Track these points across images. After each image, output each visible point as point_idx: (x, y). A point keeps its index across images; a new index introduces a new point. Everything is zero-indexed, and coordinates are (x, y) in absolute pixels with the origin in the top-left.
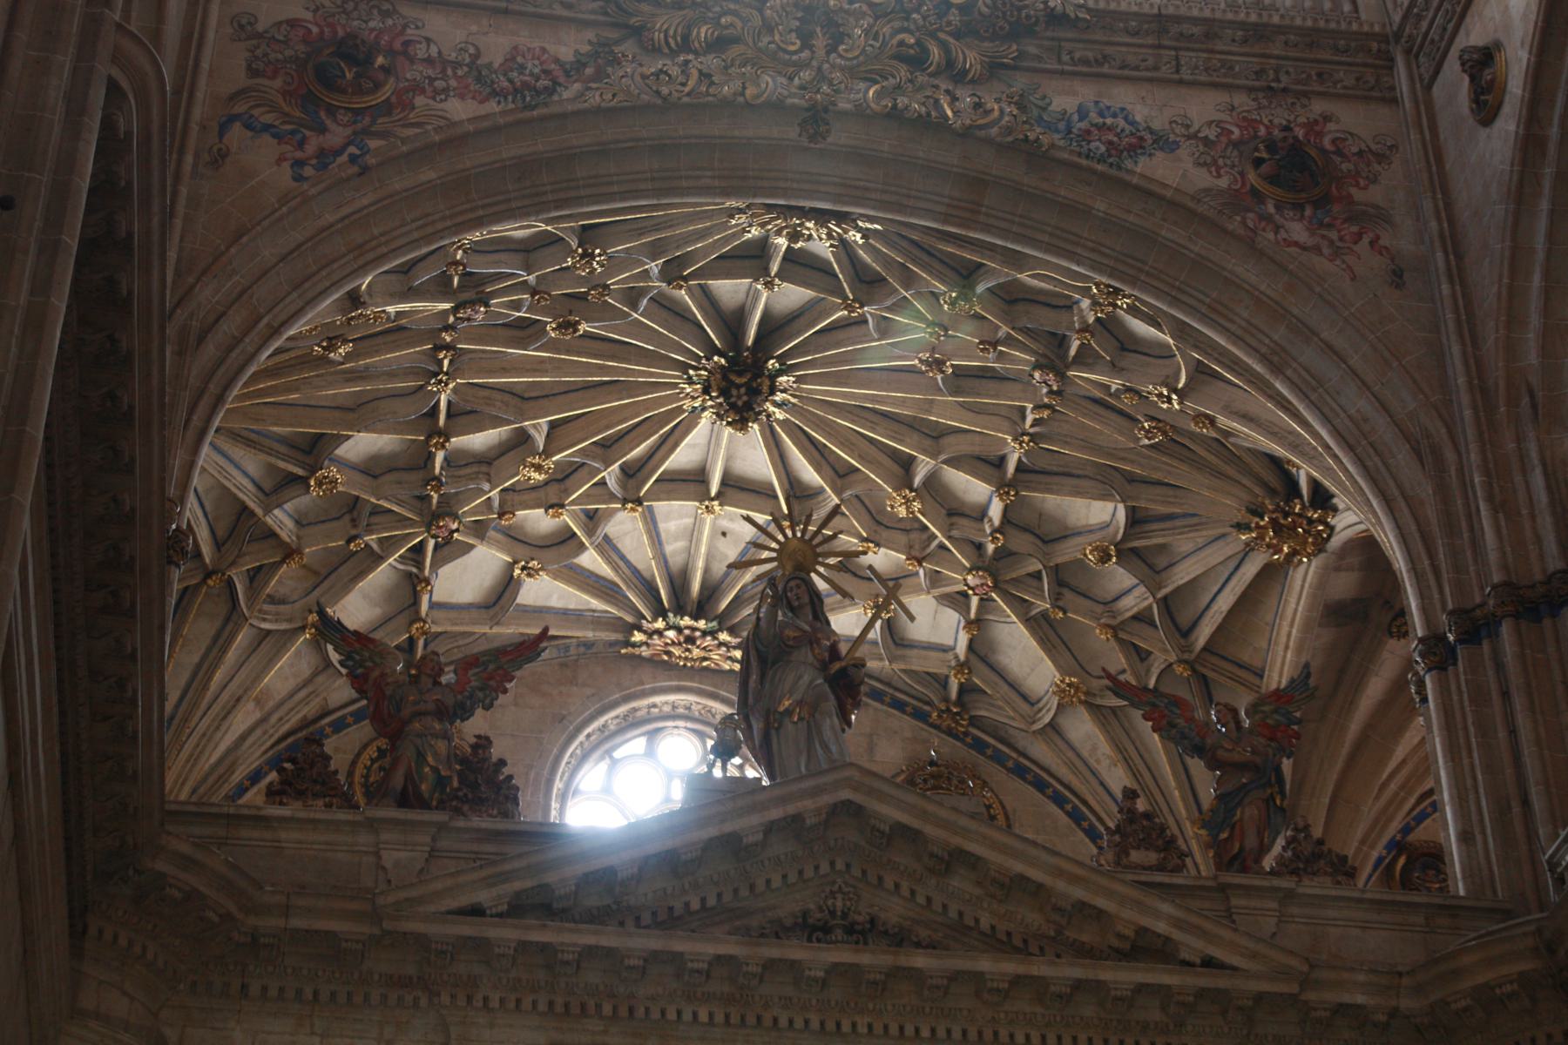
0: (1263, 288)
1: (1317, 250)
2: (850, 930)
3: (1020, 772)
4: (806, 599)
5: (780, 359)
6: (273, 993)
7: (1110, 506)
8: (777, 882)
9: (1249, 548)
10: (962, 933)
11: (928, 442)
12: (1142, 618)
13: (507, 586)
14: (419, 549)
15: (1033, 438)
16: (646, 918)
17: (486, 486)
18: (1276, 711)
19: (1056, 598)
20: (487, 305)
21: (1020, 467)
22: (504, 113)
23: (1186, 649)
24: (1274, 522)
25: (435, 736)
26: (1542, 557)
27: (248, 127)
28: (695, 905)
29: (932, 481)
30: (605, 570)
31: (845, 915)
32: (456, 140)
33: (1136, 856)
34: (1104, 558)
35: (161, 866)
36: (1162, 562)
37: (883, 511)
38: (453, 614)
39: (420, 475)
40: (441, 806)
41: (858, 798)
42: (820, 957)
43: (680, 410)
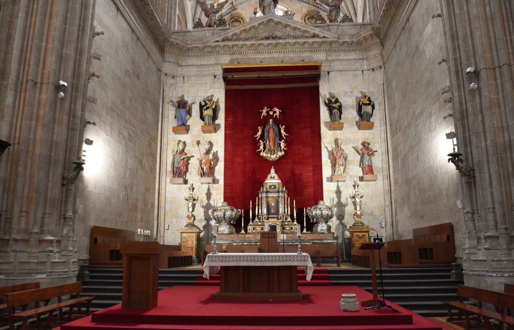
2: (273, 38)
8: (262, 32)
10: (289, 36)
16: (243, 39)
25: (213, 16)
28: (250, 37)
31: (272, 36)
33: (318, 22)
35: (172, 40)
41: (272, 18)
42: (266, 42)
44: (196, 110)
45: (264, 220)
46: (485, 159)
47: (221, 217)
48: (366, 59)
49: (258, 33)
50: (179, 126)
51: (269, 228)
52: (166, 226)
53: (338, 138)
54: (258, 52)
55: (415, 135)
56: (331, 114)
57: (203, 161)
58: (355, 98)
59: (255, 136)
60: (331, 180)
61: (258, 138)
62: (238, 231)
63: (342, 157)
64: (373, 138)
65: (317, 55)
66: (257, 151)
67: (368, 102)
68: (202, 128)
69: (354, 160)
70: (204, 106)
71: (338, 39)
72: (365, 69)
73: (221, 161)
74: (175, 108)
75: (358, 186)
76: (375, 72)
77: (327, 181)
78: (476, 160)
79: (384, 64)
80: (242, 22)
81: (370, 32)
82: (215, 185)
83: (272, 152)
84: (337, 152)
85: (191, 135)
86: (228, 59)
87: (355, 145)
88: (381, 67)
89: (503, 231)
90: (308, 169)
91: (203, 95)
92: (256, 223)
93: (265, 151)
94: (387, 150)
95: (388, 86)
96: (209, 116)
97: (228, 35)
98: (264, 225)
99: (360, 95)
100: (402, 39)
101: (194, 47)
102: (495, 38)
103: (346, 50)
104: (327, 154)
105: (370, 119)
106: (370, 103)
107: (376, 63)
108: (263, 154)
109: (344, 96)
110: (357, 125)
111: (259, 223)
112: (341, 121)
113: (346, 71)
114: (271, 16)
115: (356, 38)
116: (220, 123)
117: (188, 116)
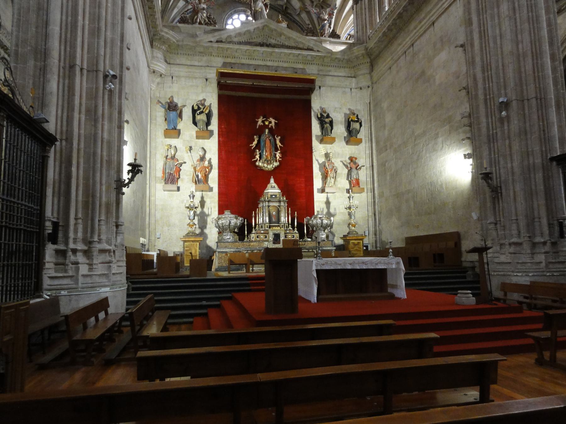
28: (244, 41)
35: (163, 34)
40: (205, 24)
44: (187, 113)
45: (267, 229)
46: (510, 178)
48: (354, 77)
51: (273, 236)
52: (158, 234)
53: (329, 152)
55: (413, 153)
56: (322, 127)
57: (198, 168)
58: (343, 115)
60: (323, 191)
61: (253, 147)
63: (333, 170)
66: (253, 160)
69: (342, 173)
72: (353, 87)
73: (215, 169)
74: (163, 110)
75: (353, 197)
76: (362, 90)
77: (318, 192)
78: (503, 179)
79: (372, 83)
81: (364, 52)
83: (268, 162)
84: (328, 165)
87: (343, 159)
88: (369, 87)
89: (526, 239)
90: (301, 180)
93: (261, 161)
94: (371, 165)
95: (376, 105)
96: (203, 121)
97: (222, 37)
98: (268, 233)
99: (348, 112)
100: (402, 62)
102: (526, 74)
104: (318, 166)
105: (357, 135)
106: (358, 121)
107: (365, 81)
108: (259, 163)
109: (334, 112)
111: (262, 232)
112: (333, 135)
116: (212, 129)
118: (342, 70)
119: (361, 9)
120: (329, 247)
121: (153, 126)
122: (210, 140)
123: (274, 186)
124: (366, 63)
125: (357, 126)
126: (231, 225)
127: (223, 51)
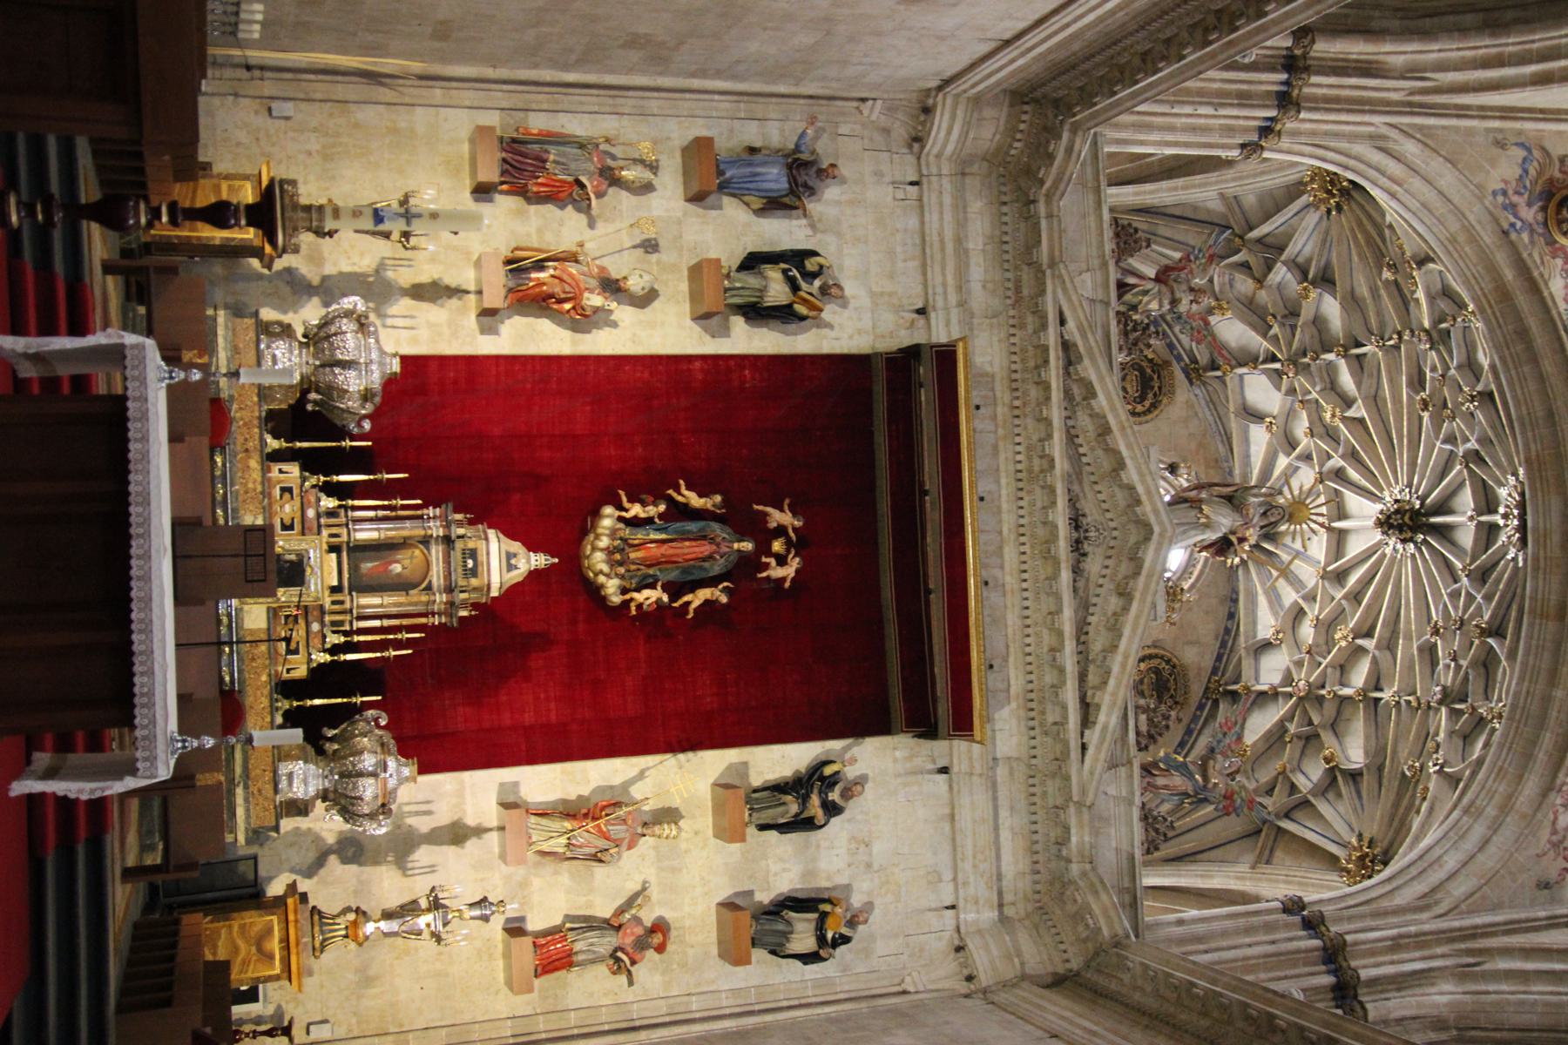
0: (1521, 799)
1: (1554, 832)
2: (1078, 541)
3: (1189, 732)
4: (1273, 520)
5: (1425, 541)
6: (1005, 219)
7: (1361, 760)
8: (1101, 497)
9: (1344, 845)
10: (1084, 607)
11: (1385, 643)
12: (1293, 788)
13: (1258, 417)
14: (1274, 359)
15: (1398, 703)
16: (1070, 423)
17: (1318, 388)
18: (1243, 800)
19: (1299, 737)
20: (1431, 348)
21: (1377, 700)
22: (1559, 314)
23: (1278, 816)
24: (1367, 854)
26: (1365, 967)
27: (1525, 160)
28: (1081, 450)
29: (1362, 650)
30: (1277, 472)
31: (1086, 538)
32: (1534, 288)
33: (1143, 717)
34: (1327, 760)
35: (1066, 136)
36: (1331, 796)
37: (1336, 625)
38: (1237, 389)
39: (1317, 347)
41: (1155, 537)
42: (1061, 516)
43: (1382, 490)
44: (784, 233)
45: (325, 533)
47: (333, 348)
48: (1003, 920)
49: (1096, 483)
50: (718, 166)
51: (293, 557)
52: (288, 108)
53: (681, 823)
54: (1020, 485)
56: (779, 788)
57: (573, 269)
58: (845, 881)
59: (682, 482)
61: (675, 495)
62: (277, 422)
63: (603, 844)
64: (684, 965)
65: (1014, 722)
66: (622, 493)
67: (830, 935)
68: (709, 261)
70: (804, 267)
71: (1079, 804)
72: (962, 916)
73: (574, 343)
75: (485, 919)
76: (953, 955)
79: (985, 991)
80: (1139, 408)
81: (1106, 932)
82: (473, 316)
83: (617, 556)
85: (679, 214)
86: (991, 363)
87: (654, 892)
88: (969, 978)
91: (847, 262)
92: (313, 499)
93: (621, 525)
94: (637, 1023)
95: (896, 1012)
96: (761, 291)
97: (1086, 362)
99: (857, 901)
101: (1038, 224)
103: (1035, 837)
104: (617, 781)
105: (763, 946)
106: (826, 945)
107: (987, 961)
108: (608, 516)
109: (853, 838)
110: (737, 894)
111: (311, 513)
112: (751, 831)
113: (954, 840)
114: (1161, 535)
115: (1084, 874)
116: (733, 334)
117: (758, 204)
118: (1024, 864)
119: (1269, 927)
120: (248, 816)
121: (725, 104)
122: (688, 322)
123: (516, 568)
124: (1065, 956)
125: (803, 940)
126: (337, 370)
127: (1037, 367)
